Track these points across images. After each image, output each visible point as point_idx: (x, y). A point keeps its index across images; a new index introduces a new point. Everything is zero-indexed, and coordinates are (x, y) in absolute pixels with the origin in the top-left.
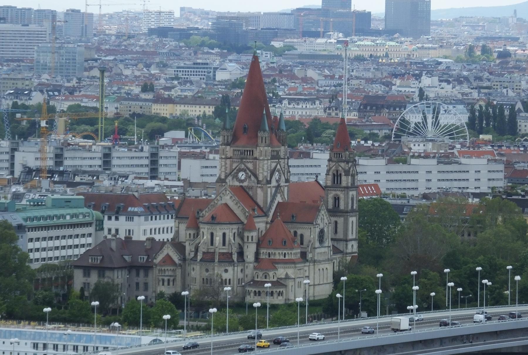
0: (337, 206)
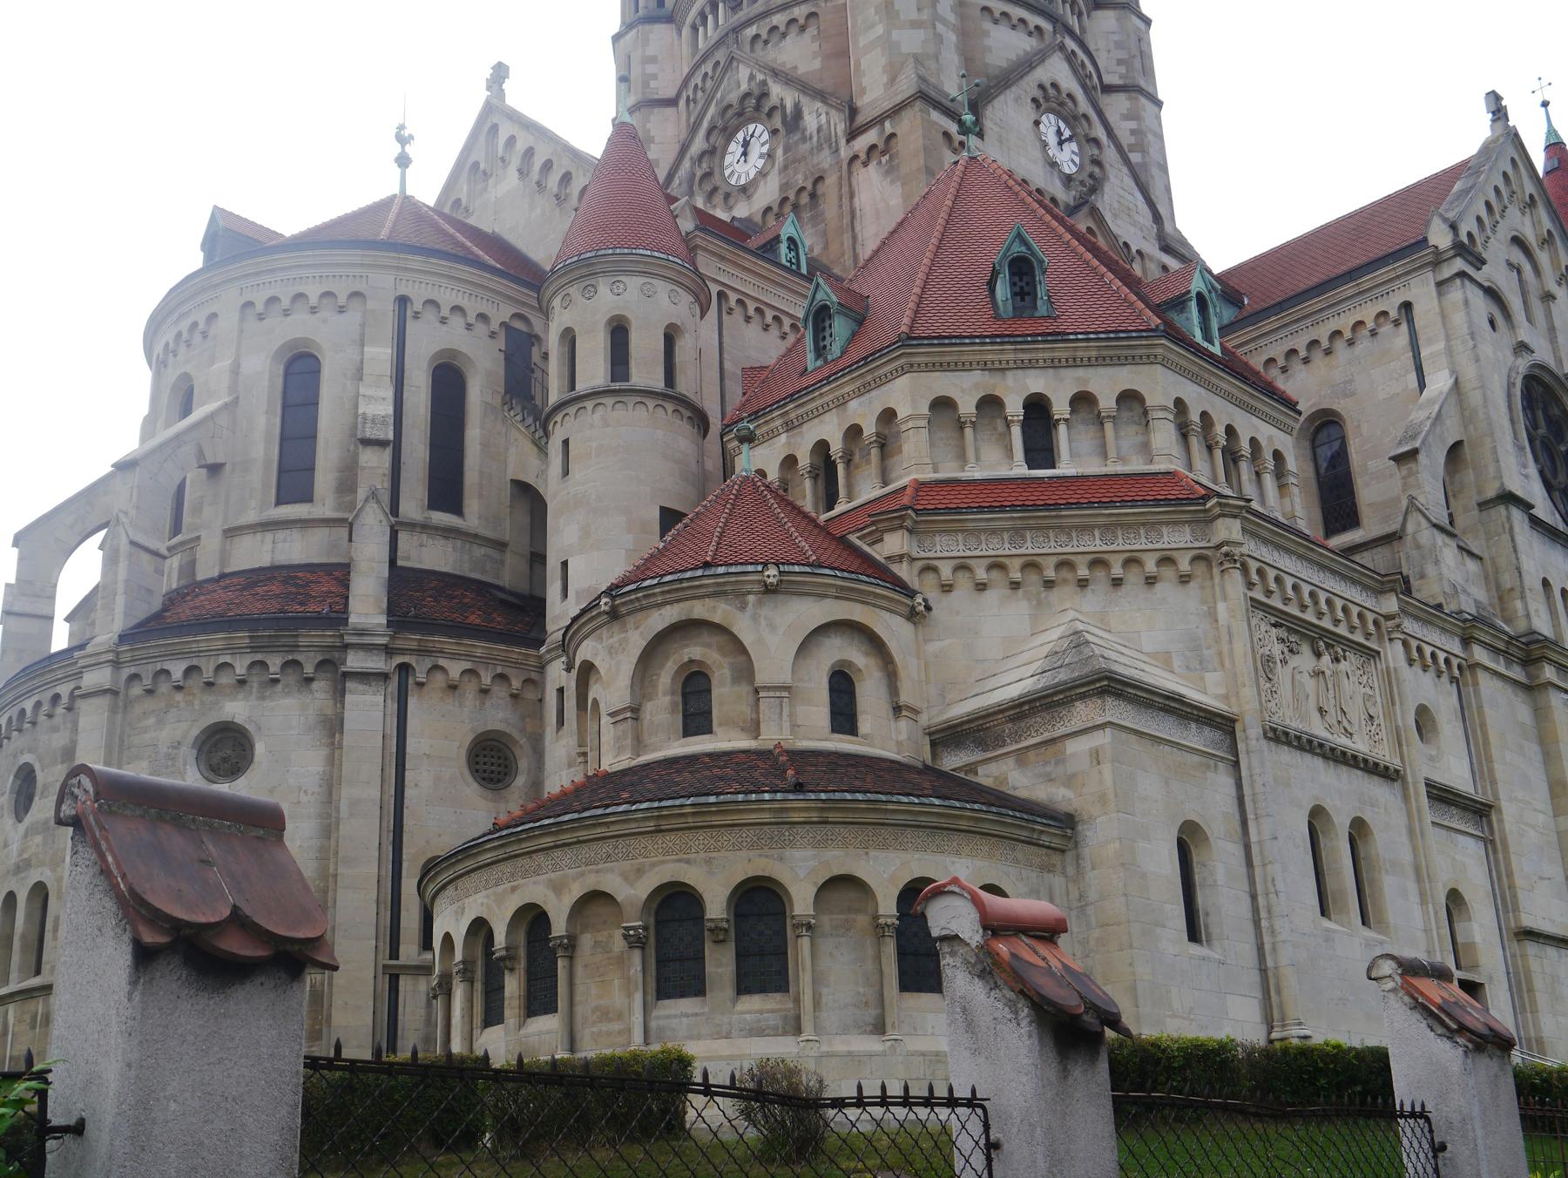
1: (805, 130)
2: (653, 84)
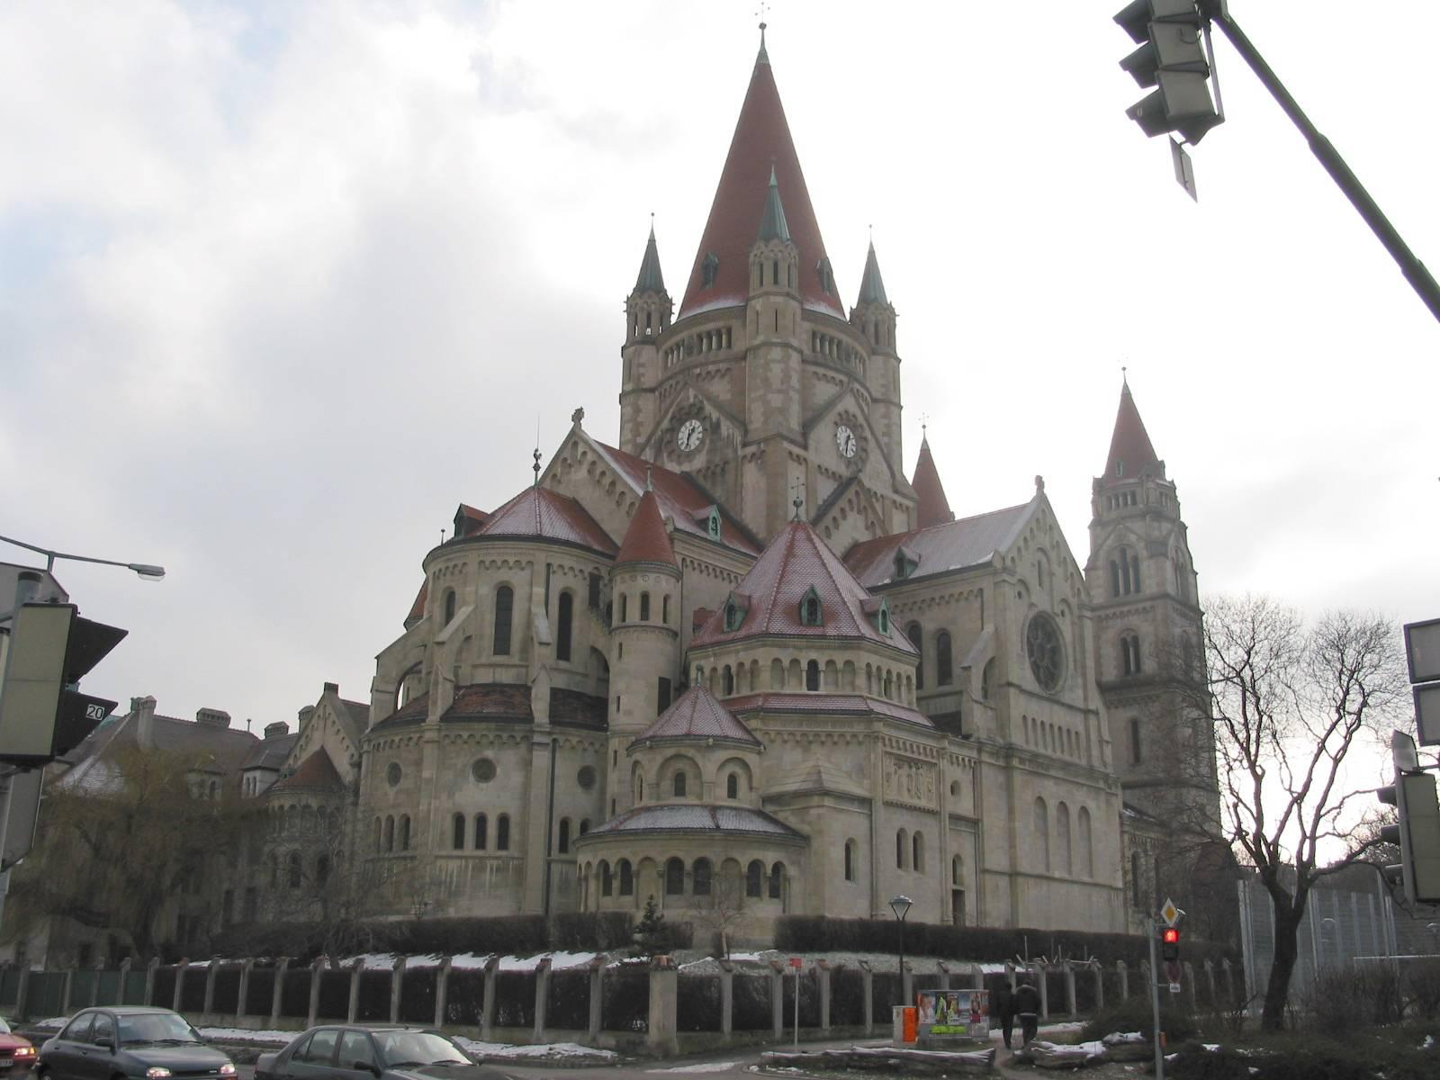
0: (1133, 668)
1: (721, 434)
2: (642, 379)
